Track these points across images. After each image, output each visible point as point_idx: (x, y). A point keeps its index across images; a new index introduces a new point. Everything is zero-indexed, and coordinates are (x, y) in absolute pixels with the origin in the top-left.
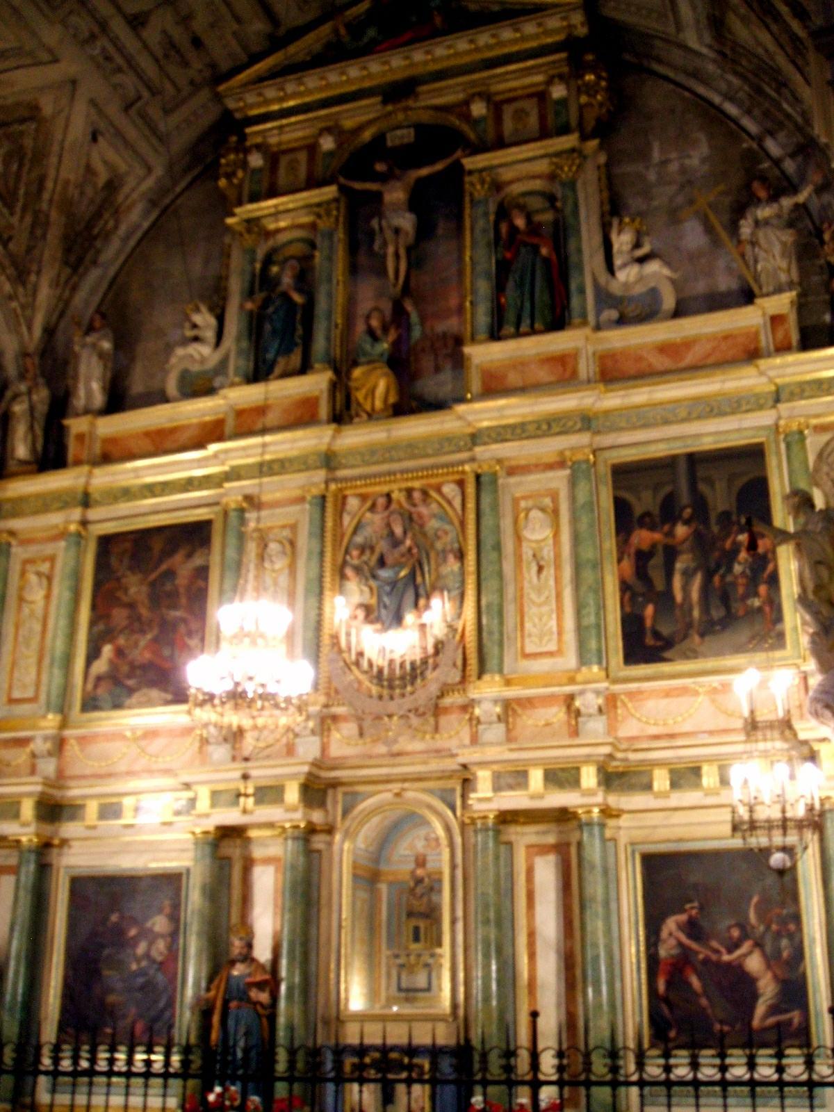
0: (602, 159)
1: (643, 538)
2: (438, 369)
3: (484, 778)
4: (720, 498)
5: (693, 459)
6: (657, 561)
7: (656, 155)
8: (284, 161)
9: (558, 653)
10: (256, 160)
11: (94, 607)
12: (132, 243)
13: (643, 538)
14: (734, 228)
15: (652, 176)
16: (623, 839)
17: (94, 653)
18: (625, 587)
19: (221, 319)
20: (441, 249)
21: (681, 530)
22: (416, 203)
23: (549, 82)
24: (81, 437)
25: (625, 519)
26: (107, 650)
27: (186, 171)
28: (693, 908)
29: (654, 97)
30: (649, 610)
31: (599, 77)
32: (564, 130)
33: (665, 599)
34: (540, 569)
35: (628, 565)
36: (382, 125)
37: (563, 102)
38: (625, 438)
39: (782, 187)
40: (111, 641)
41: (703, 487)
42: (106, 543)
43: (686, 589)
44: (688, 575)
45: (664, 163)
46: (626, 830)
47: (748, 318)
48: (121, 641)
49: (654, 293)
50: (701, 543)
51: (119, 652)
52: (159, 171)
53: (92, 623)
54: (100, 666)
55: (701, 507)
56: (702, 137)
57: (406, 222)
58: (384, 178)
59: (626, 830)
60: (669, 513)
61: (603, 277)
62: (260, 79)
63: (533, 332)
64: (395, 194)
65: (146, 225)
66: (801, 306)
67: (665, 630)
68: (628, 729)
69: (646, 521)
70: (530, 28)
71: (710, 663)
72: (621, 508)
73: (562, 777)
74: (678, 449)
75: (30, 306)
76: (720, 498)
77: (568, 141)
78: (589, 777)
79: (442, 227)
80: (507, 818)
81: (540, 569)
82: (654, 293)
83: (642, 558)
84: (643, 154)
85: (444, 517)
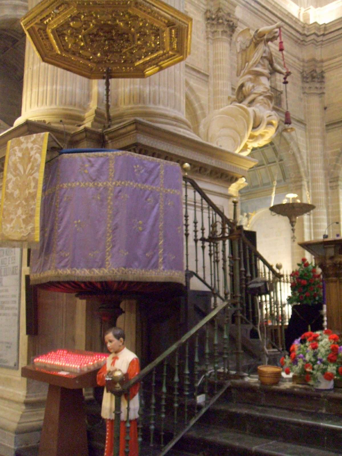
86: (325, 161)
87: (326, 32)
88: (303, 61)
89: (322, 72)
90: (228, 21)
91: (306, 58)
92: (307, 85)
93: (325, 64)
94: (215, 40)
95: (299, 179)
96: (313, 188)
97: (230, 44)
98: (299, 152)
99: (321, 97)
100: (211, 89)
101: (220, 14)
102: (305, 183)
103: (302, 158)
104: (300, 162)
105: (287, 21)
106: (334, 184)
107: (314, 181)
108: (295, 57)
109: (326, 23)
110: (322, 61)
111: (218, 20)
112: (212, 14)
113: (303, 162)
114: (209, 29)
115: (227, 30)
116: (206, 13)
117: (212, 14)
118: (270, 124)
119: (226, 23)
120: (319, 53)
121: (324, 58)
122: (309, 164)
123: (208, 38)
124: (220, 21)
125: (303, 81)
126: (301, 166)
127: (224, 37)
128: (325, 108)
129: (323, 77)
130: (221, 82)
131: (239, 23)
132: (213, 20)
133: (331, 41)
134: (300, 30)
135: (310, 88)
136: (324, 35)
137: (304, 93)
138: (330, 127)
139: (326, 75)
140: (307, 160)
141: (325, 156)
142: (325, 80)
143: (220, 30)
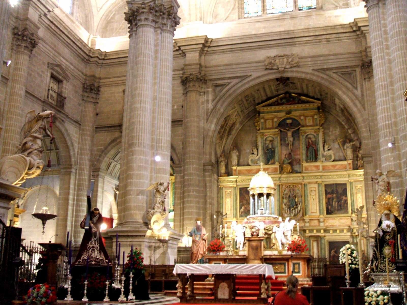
0: (323, 130)
1: (329, 196)
2: (296, 165)
3: (307, 232)
4: (340, 191)
5: (337, 185)
6: (331, 200)
7: (331, 130)
8: (268, 121)
9: (316, 212)
11: (240, 200)
12: (238, 131)
13: (329, 196)
14: (343, 147)
15: (330, 133)
16: (326, 239)
17: (240, 208)
18: (326, 203)
19: (258, 150)
20: (296, 143)
21: (334, 195)
22: (293, 136)
23: (315, 114)
24: (235, 170)
25: (326, 193)
26: (243, 207)
27: (247, 118)
28: (335, 249)
29: (331, 118)
30: (330, 207)
32: (317, 125)
33: (332, 205)
34: (314, 200)
35: (327, 200)
36: (285, 117)
37: (316, 119)
38: (326, 180)
39: (351, 141)
40: (244, 206)
41: (338, 189)
42: (240, 189)
43: (335, 204)
44: (335, 202)
45: (332, 131)
46: (327, 238)
47: (345, 163)
48: (245, 206)
49: (330, 156)
50: (338, 197)
51: (245, 208)
52: (242, 118)
53: (240, 203)
54: (242, 210)
55: (337, 192)
56: (338, 127)
57: (291, 139)
58: (288, 130)
59: (327, 238)
60: (332, 193)
61: (323, 152)
62: (263, 106)
63: (312, 162)
64: (290, 134)
65: (240, 128)
66: (353, 162)
67: (332, 210)
68: (327, 224)
69: (329, 193)
70: (311, 105)
71: (338, 215)
72: (326, 191)
73: (318, 231)
74: (335, 183)
75: (222, 144)
76: (340, 191)
77: (317, 127)
78: (322, 231)
79: (296, 139)
80: (310, 236)
81: (314, 200)
82: (330, 156)
83: (329, 199)
84: (329, 129)
85: (299, 190)
86: (92, 155)
87: (106, 58)
88: (86, 75)
89: (99, 87)
90: (31, 39)
91: (89, 73)
92: (86, 94)
93: (101, 81)
94: (18, 52)
95: (70, 167)
96: (80, 175)
97: (30, 57)
98: (72, 144)
99: (95, 105)
100: (8, 89)
101: (26, 33)
102: (73, 170)
103: (74, 151)
104: (72, 153)
105: (78, 44)
106: (96, 174)
107: (81, 169)
108: (80, 71)
109: (107, 51)
110: (100, 78)
111: (23, 37)
112: (19, 31)
113: (74, 154)
114: (14, 42)
115: (29, 46)
116: (14, 29)
117: (19, 31)
118: (38, 167)
119: (29, 40)
120: (99, 72)
121: (102, 76)
122: (79, 156)
123: (12, 49)
124: (25, 38)
125: (83, 91)
126: (72, 156)
127: (26, 51)
128: (97, 114)
129: (99, 91)
130: (17, 86)
131: (40, 41)
132: (19, 35)
133: (109, 65)
134: (87, 53)
135: (88, 97)
136: (104, 59)
137: (83, 100)
138: (98, 130)
139: (102, 89)
140: (78, 152)
141: (92, 151)
142: (100, 93)
143: (24, 44)
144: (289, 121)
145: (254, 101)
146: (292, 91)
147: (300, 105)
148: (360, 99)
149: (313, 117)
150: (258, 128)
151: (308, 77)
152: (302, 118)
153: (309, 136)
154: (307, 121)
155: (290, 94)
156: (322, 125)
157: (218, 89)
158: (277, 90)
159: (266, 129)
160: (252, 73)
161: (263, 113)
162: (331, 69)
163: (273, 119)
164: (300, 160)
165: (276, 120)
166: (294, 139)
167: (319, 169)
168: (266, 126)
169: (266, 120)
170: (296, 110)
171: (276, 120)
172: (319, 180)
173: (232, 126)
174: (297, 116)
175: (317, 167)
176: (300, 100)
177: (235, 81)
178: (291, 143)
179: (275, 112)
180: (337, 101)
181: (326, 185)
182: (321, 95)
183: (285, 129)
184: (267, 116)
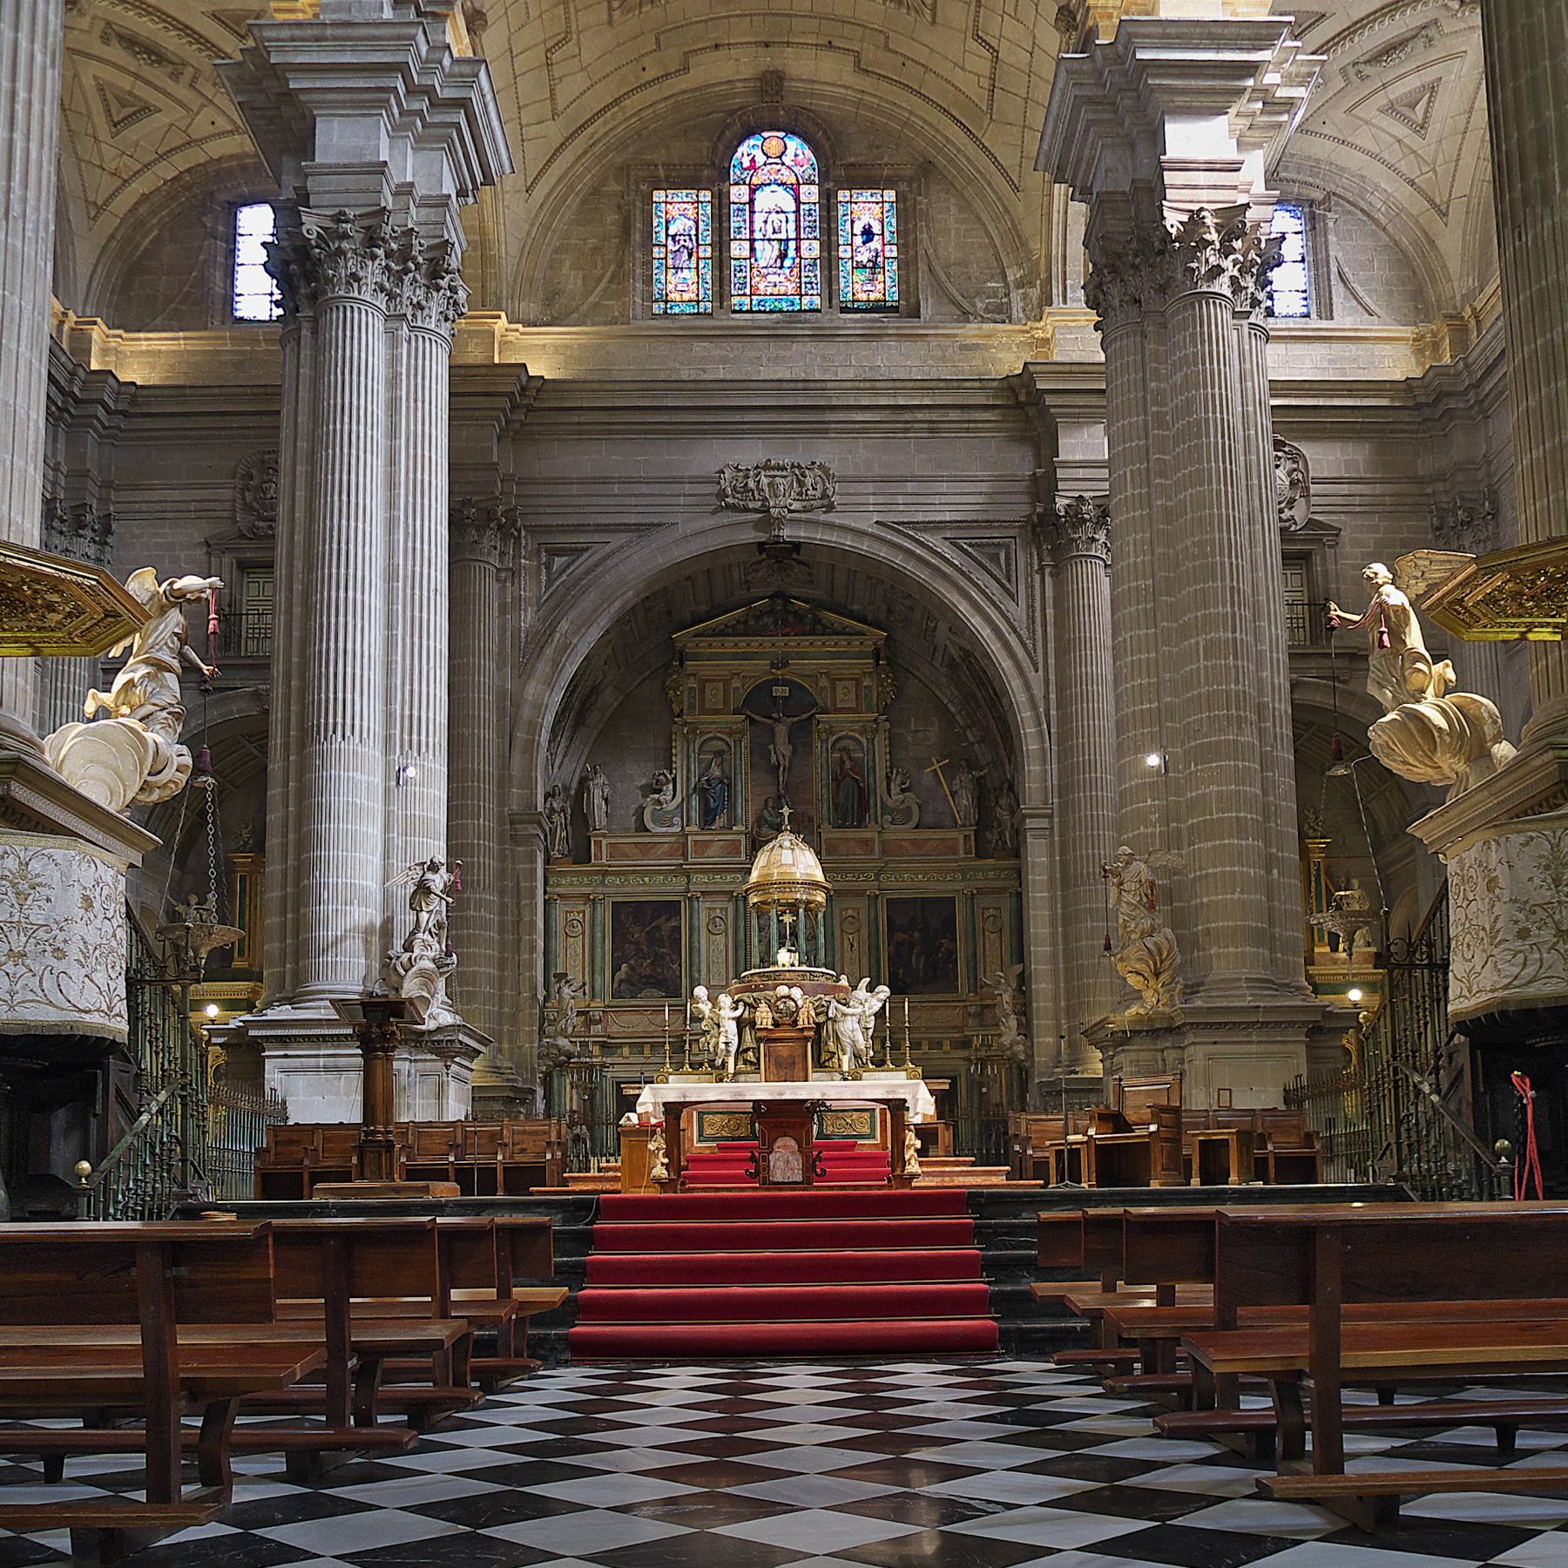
1: (902, 936)
10: (692, 683)
13: (902, 936)
22: (791, 739)
31: (888, 677)
32: (869, 710)
61: (886, 797)
64: (781, 731)
144: (781, 691)
145: (669, 613)
146: (795, 591)
147: (818, 640)
148: (1024, 633)
149: (858, 681)
150: (676, 709)
151: (865, 546)
152: (824, 682)
153: (842, 744)
154: (839, 692)
155: (787, 599)
156: (885, 710)
157: (559, 561)
158: (748, 584)
159: (704, 711)
160: (679, 519)
161: (696, 657)
162: (937, 526)
163: (726, 683)
164: (811, 819)
165: (736, 683)
166: (794, 752)
167: (872, 852)
168: (702, 701)
169: (703, 683)
170: (802, 656)
171: (736, 683)
172: (871, 887)
173: (588, 697)
174: (800, 676)
175: (866, 844)
176: (818, 621)
177: (617, 540)
178: (784, 763)
179: (735, 657)
180: (942, 633)
181: (891, 903)
182: (890, 611)
183: (770, 718)
184: (707, 668)
